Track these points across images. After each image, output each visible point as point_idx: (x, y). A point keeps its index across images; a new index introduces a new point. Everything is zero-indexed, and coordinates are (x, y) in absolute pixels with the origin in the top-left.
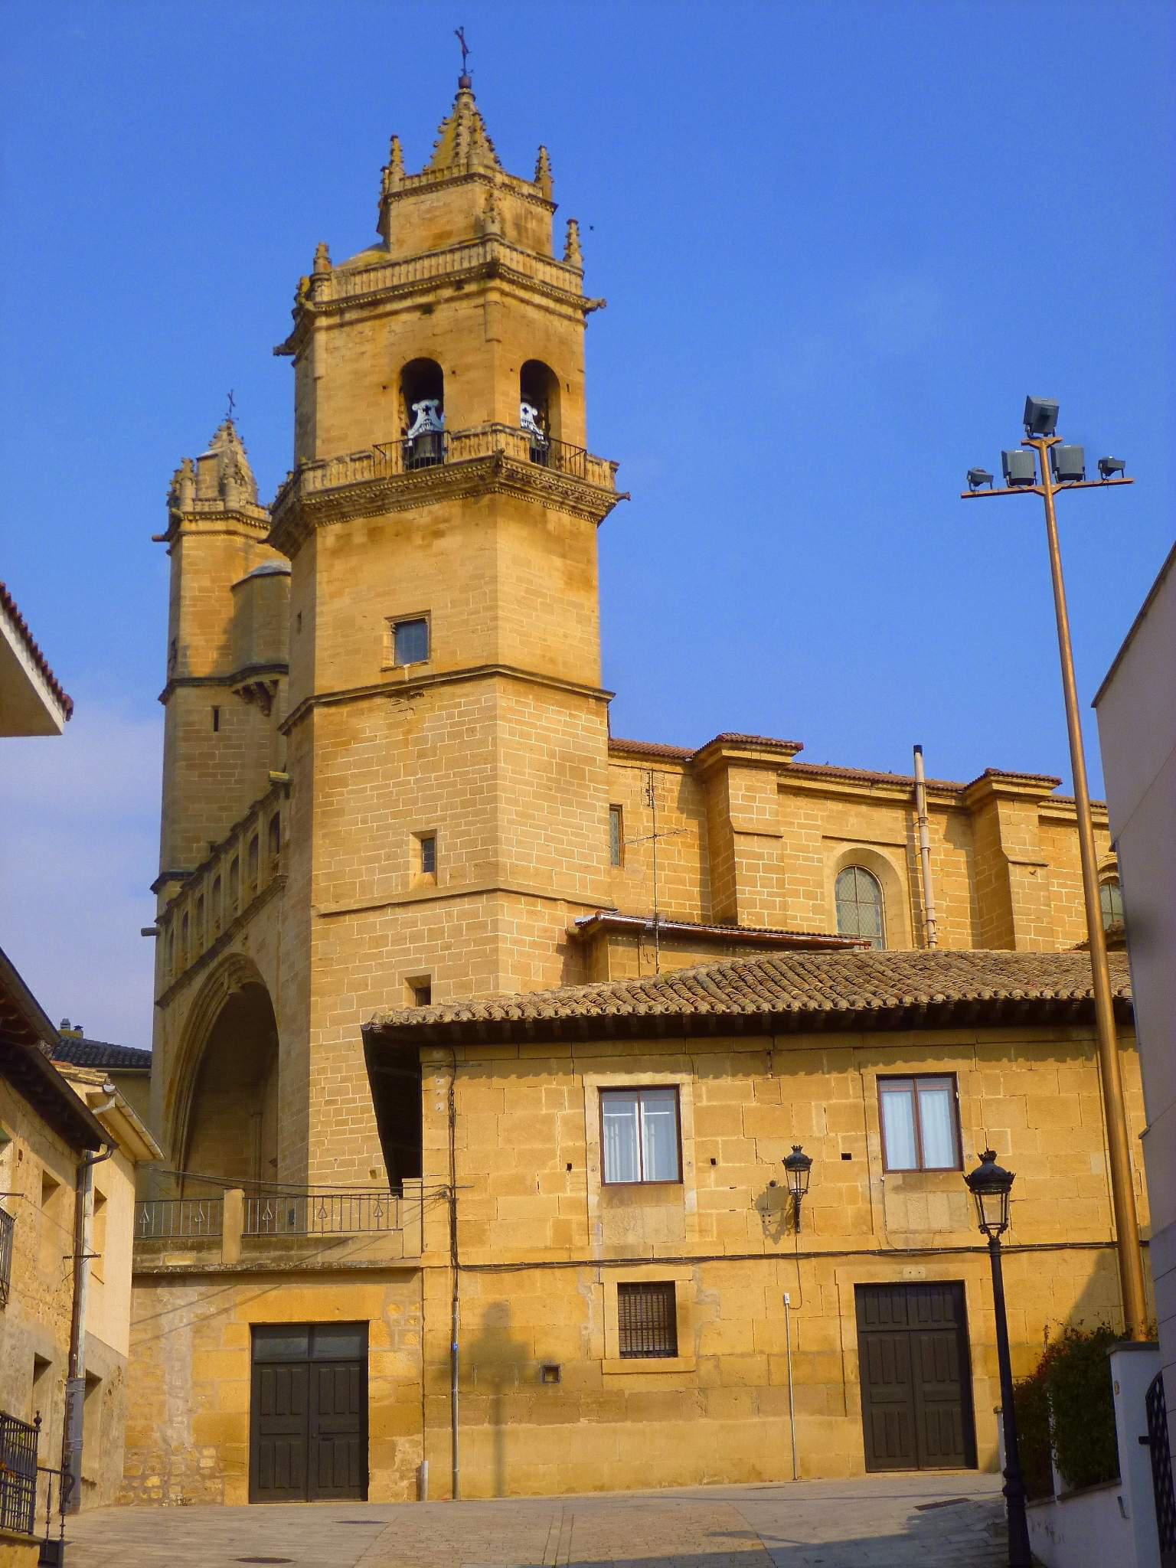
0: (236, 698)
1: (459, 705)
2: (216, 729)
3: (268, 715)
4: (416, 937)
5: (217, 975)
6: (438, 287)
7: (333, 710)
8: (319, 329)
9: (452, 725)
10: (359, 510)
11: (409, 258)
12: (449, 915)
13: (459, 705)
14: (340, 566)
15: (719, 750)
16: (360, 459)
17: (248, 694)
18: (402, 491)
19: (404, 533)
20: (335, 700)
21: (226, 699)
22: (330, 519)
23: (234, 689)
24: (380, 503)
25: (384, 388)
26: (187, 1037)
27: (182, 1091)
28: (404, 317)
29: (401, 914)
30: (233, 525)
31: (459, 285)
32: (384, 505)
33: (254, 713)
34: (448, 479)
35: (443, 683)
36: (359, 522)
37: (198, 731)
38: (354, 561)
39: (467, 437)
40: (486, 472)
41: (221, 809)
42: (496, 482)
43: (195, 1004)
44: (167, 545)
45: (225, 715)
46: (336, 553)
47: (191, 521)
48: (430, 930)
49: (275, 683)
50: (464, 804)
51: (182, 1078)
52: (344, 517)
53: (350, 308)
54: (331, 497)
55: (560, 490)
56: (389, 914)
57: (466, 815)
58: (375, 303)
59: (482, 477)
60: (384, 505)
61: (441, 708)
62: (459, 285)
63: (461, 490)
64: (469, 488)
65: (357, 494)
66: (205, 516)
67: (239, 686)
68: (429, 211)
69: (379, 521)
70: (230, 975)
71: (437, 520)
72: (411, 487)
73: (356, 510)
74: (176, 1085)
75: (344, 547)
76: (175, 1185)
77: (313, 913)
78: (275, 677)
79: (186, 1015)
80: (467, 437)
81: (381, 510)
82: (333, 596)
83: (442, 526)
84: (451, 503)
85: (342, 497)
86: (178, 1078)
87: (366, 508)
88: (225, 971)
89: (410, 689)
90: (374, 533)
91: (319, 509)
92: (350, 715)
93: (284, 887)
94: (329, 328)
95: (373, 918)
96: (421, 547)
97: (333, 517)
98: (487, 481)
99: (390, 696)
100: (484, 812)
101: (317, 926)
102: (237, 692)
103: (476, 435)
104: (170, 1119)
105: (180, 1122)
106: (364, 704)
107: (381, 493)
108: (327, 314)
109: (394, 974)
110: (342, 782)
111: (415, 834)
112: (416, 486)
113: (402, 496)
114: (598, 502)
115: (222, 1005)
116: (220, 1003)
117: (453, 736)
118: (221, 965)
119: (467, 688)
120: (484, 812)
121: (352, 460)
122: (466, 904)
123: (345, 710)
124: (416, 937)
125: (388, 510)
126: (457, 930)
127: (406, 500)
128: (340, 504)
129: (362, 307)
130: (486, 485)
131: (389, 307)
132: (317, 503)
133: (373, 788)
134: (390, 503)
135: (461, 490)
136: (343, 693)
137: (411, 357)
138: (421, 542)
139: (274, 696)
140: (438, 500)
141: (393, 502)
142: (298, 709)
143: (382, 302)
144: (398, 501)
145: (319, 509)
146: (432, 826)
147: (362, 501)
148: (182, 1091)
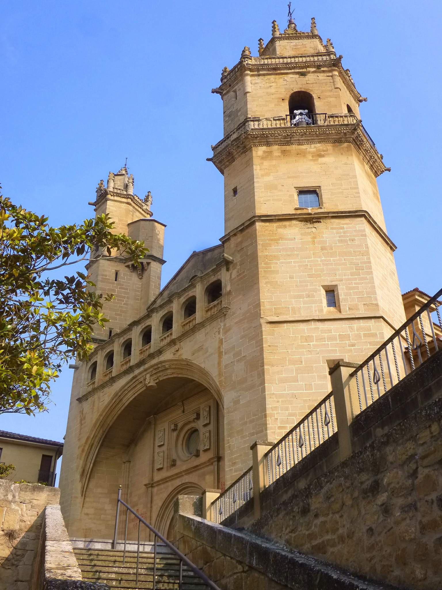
0: (127, 269)
1: (343, 228)
2: (116, 280)
3: (141, 279)
4: (330, 339)
5: (139, 377)
6: (308, 67)
7: (267, 224)
8: (247, 75)
9: (340, 237)
10: (277, 141)
11: (291, 56)
12: (351, 328)
13: (343, 228)
14: (266, 163)
15: (414, 295)
16: (278, 120)
17: (134, 268)
18: (302, 135)
19: (302, 154)
20: (268, 219)
21: (122, 269)
22: (260, 145)
23: (126, 264)
24: (289, 140)
25: (283, 100)
26: (104, 414)
27: (93, 444)
28: (291, 76)
29: (320, 325)
30: (129, 201)
31: (319, 67)
32: (290, 140)
33: (134, 277)
34: (328, 132)
35: (333, 217)
36: (276, 147)
37: (109, 279)
38: (274, 162)
39: (337, 117)
40: (348, 132)
41: (116, 314)
42: (351, 138)
43: (116, 395)
44: (94, 207)
45: (121, 275)
46: (263, 158)
47: (111, 195)
48: (325, 341)
49: (148, 264)
50: (352, 274)
51: (95, 436)
52: (268, 144)
53: (263, 69)
54: (264, 133)
55: (370, 154)
56: (313, 325)
57: (356, 279)
58: (275, 69)
59: (345, 134)
60: (290, 140)
61: (332, 228)
62: (319, 67)
63: (332, 139)
64: (337, 138)
65: (278, 133)
66: (118, 195)
67: (130, 263)
68: (295, 46)
69: (288, 148)
70: (151, 376)
71: (319, 150)
72: (307, 133)
73: (275, 141)
74: (90, 439)
75: (268, 155)
76: (80, 495)
77: (262, 321)
78: (149, 261)
79: (106, 403)
80: (337, 117)
81: (289, 143)
82: (263, 176)
83: (322, 153)
84: (326, 144)
85: (270, 134)
86: (92, 436)
87: (281, 141)
88: (148, 373)
89: (313, 218)
90: (284, 152)
91: (256, 138)
92: (278, 227)
93: (225, 315)
94: (252, 76)
95: (302, 326)
96: (311, 160)
97: (262, 143)
98: (347, 137)
99: (300, 221)
100: (366, 279)
101: (266, 328)
102: (128, 266)
103: (341, 117)
104: (83, 458)
105: (89, 460)
106: (287, 223)
107: (291, 134)
108: (251, 70)
109: (319, 357)
110: (277, 258)
111: (324, 287)
112: (310, 134)
113: (302, 137)
114: (379, 168)
115: (136, 395)
116: (134, 394)
117: (341, 241)
118: (145, 370)
119: (347, 221)
120: (366, 279)
121: (274, 120)
122: (362, 323)
123: (275, 225)
124: (330, 339)
125: (292, 144)
126: (359, 336)
127: (302, 140)
128: (267, 137)
129: (268, 70)
130: (346, 138)
131: (282, 71)
132: (256, 134)
133: (295, 262)
134: (294, 140)
135: (332, 139)
136: (275, 216)
137: (296, 90)
138: (311, 158)
139: (146, 270)
140: (319, 142)
141: (296, 140)
142: (243, 224)
143: (279, 69)
144: (299, 140)
145: (256, 138)
146: (334, 283)
147: (280, 137)
148: (93, 444)
